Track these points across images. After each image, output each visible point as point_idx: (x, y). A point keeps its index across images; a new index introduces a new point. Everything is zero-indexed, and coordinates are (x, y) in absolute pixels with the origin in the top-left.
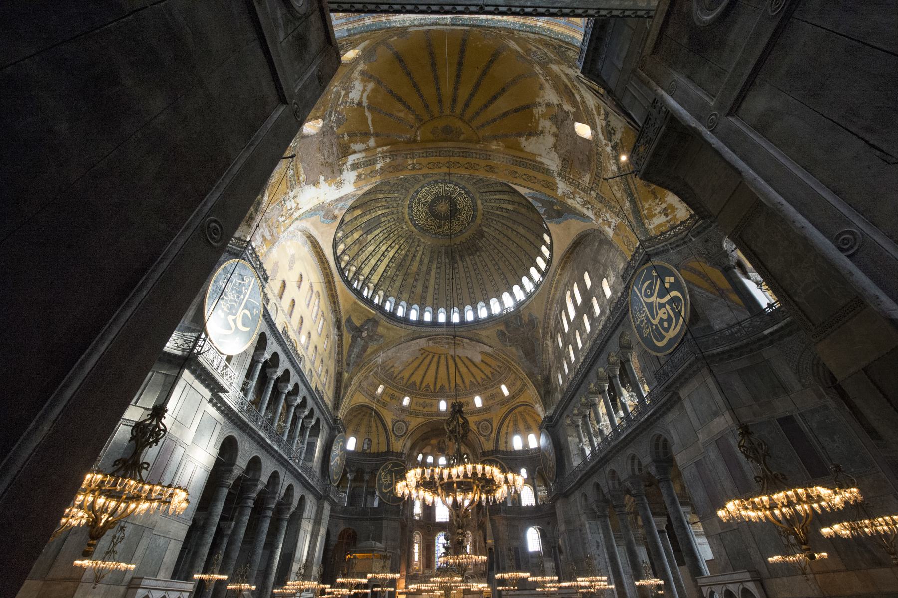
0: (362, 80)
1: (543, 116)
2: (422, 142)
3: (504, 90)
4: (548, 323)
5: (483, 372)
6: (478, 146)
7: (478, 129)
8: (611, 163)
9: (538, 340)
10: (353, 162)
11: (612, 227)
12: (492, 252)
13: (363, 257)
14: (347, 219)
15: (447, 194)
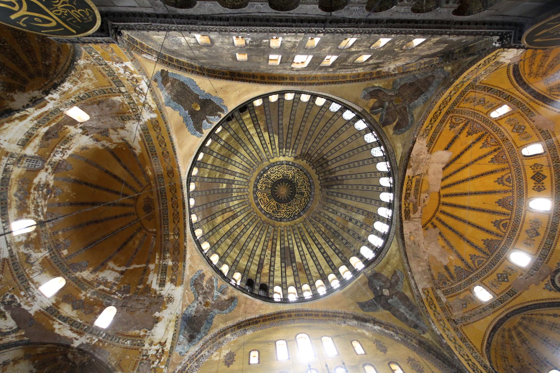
0: (102, 271)
1: (111, 141)
2: (155, 228)
3: (107, 172)
4: (364, 75)
5: (470, 146)
6: (153, 185)
7: (142, 186)
8: (66, 89)
9: (394, 83)
10: (158, 285)
11: (124, 65)
12: (321, 144)
13: (313, 270)
14: (265, 280)
15: (270, 188)
